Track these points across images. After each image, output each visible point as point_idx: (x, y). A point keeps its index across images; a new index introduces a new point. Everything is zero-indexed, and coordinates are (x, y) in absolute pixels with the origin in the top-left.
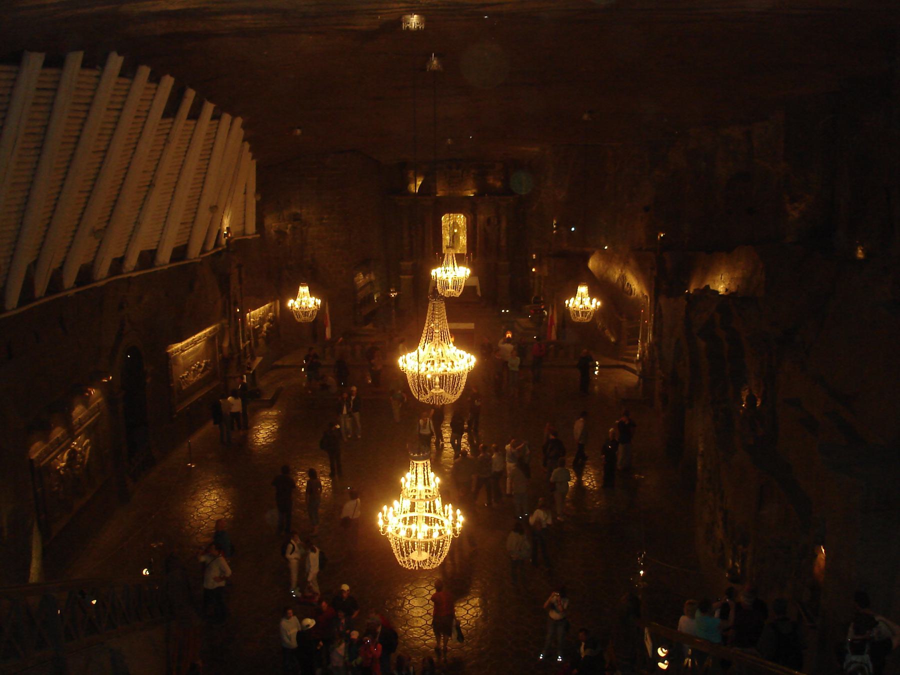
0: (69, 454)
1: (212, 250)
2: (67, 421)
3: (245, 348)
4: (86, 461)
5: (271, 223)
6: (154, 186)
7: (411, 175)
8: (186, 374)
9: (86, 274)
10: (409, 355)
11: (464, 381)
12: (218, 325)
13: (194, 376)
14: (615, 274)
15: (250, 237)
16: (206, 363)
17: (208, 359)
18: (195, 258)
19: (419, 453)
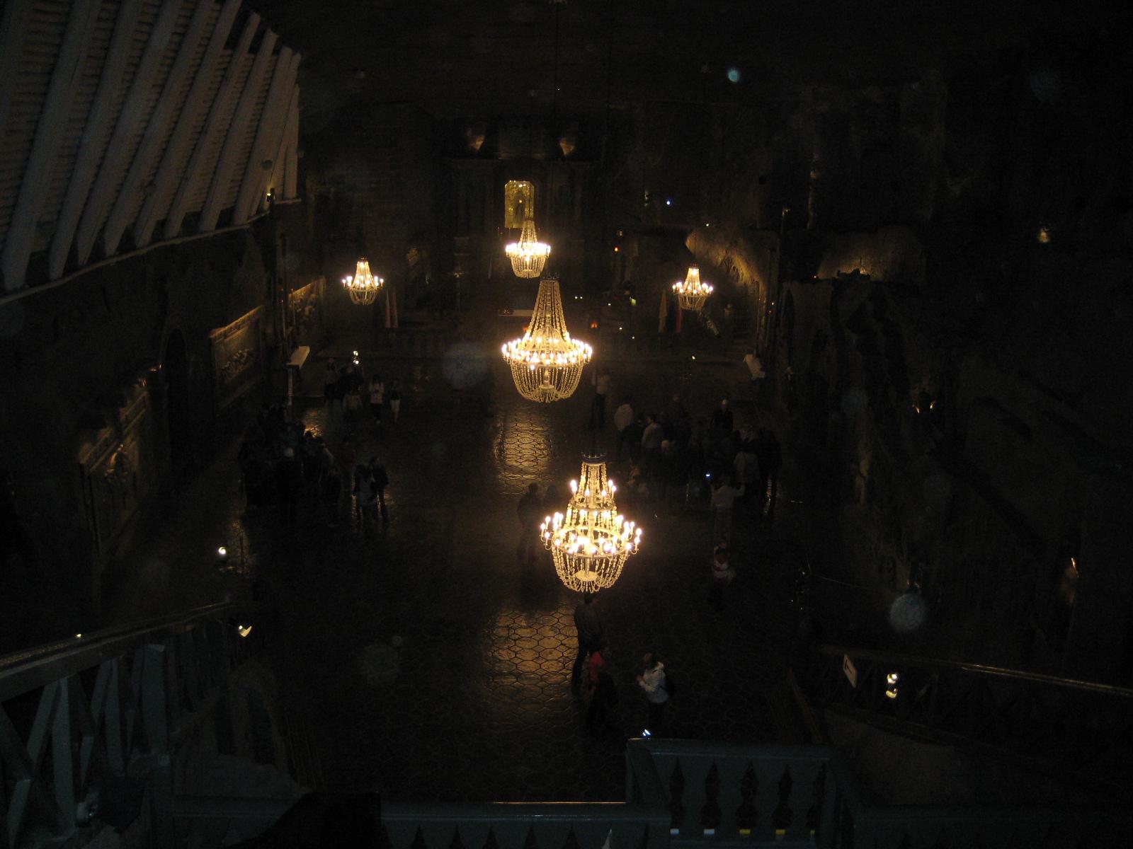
0: (116, 459)
1: (254, 216)
6: (206, 133)
9: (128, 241)
10: (515, 342)
11: (579, 375)
14: (719, 256)
15: (290, 202)
16: (250, 354)
18: (243, 225)
19: (593, 455)
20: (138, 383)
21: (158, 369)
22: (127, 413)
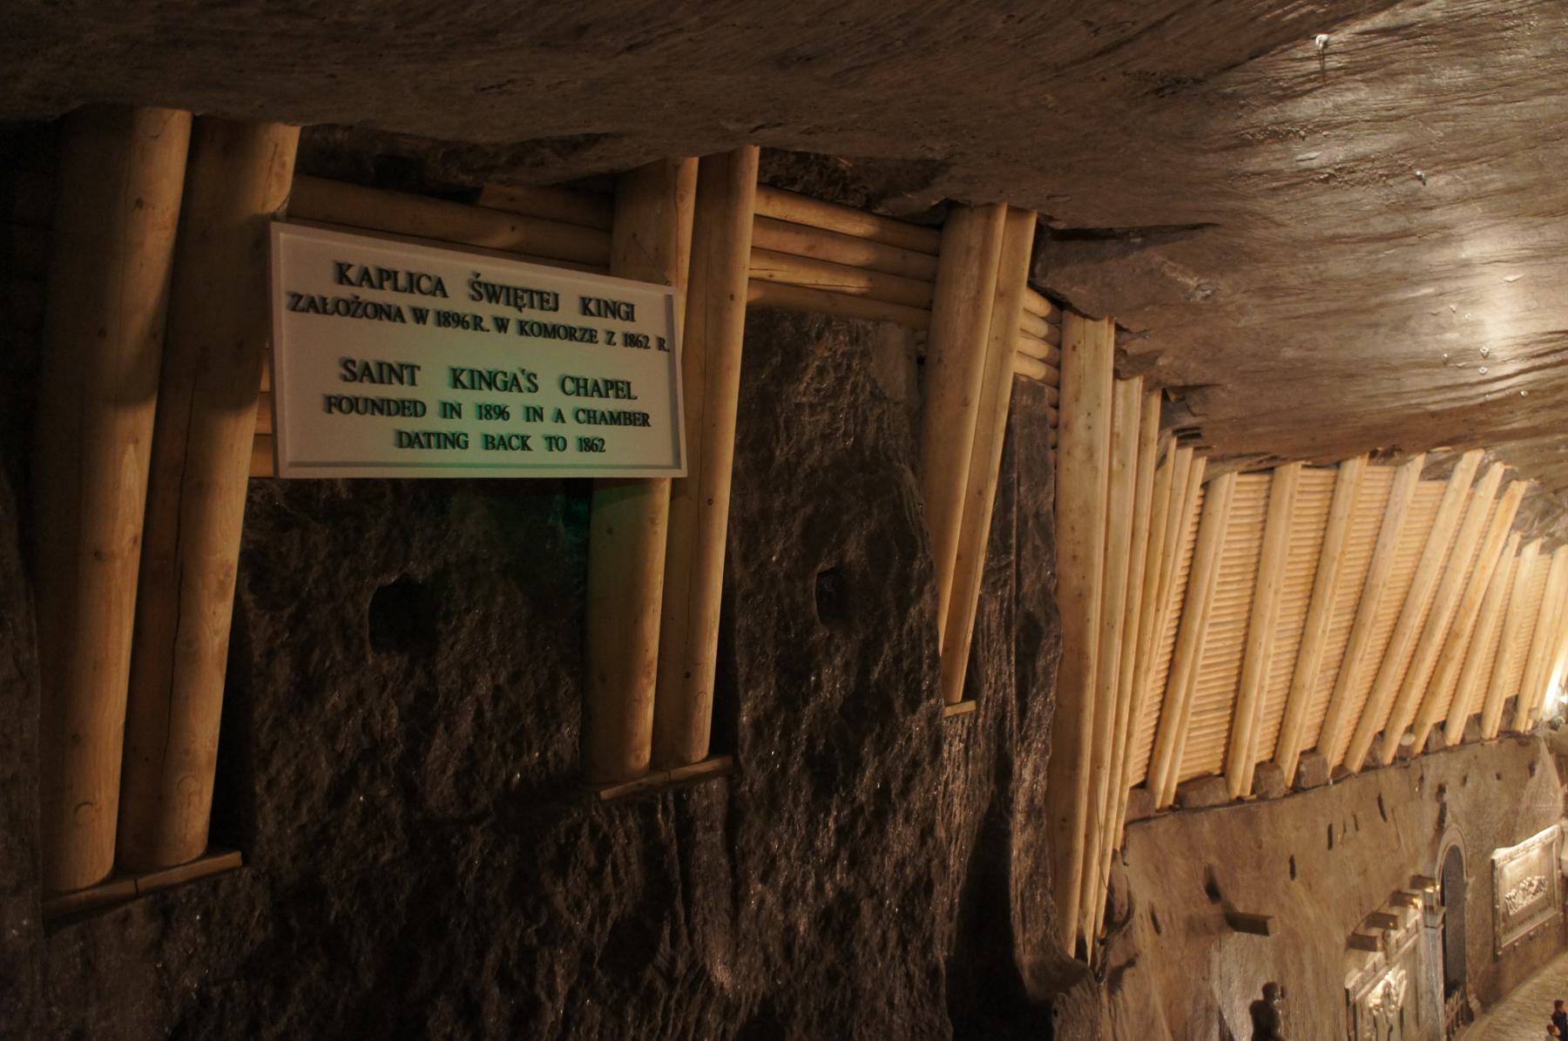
2: (1385, 938)
20: (1413, 903)
21: (1435, 890)
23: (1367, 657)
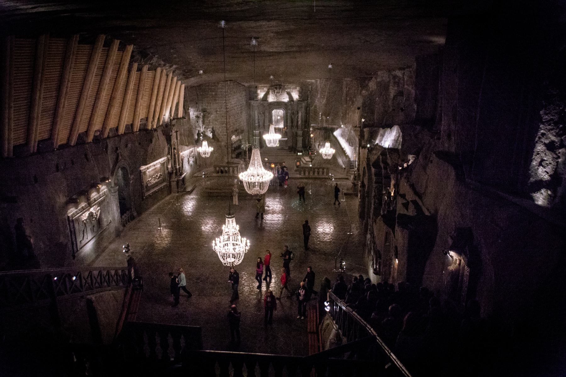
0: (89, 214)
2: (88, 199)
3: (179, 168)
4: (98, 218)
5: (192, 113)
7: (259, 91)
8: (150, 179)
12: (165, 158)
13: (154, 180)
17: (161, 172)
20: (98, 186)
22: (95, 197)
23: (66, 107)
